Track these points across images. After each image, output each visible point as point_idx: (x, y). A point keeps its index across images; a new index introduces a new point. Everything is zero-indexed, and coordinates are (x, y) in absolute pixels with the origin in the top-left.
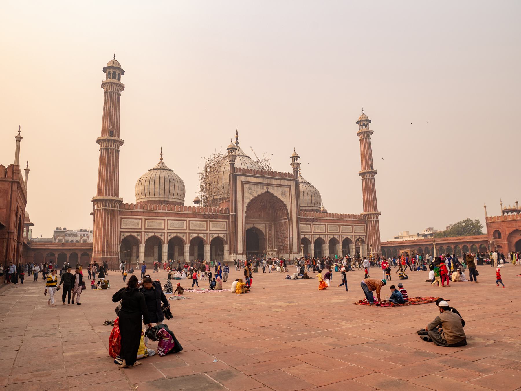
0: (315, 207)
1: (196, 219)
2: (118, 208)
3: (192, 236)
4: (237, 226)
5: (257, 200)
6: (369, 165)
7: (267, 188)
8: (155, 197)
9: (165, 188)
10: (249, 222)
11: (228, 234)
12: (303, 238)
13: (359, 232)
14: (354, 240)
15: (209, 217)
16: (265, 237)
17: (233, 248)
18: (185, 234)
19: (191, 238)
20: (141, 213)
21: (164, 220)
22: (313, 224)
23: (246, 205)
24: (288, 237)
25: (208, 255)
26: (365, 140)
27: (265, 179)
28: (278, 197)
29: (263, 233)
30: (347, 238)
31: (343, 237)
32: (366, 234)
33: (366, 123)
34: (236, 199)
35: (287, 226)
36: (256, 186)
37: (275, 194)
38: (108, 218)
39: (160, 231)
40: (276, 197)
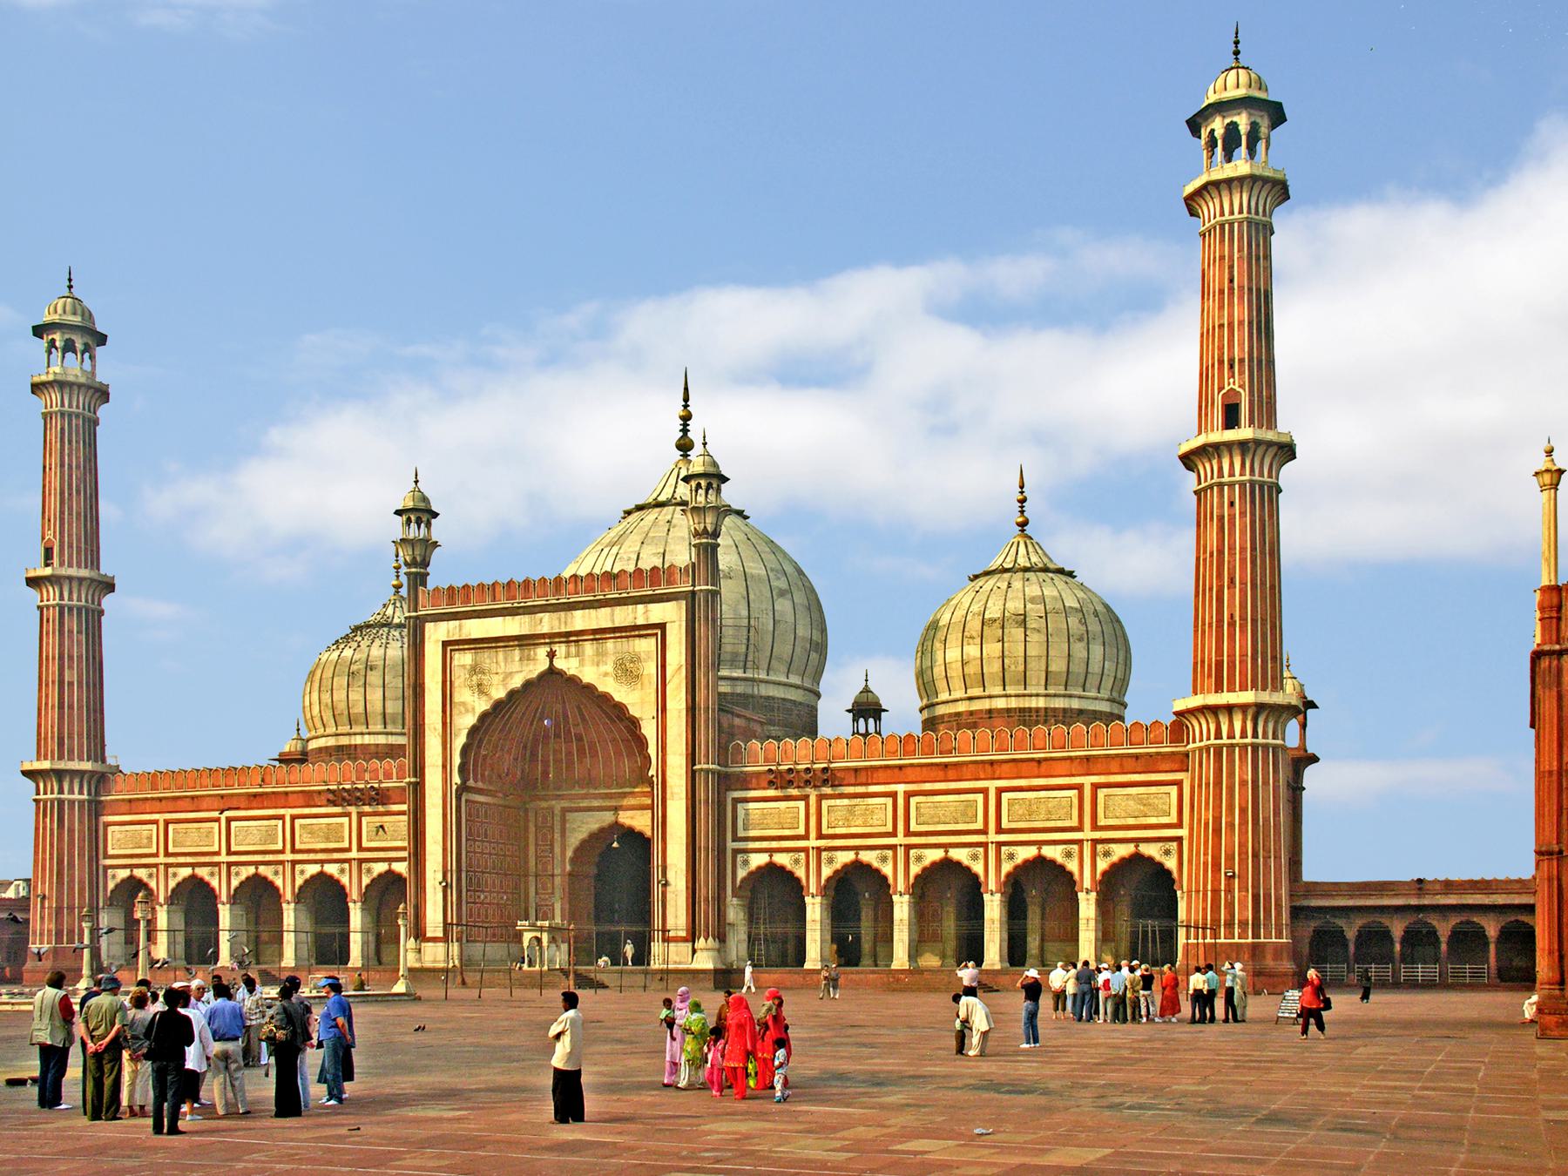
0: (1006, 696)
2: (81, 792)
7: (551, 655)
10: (596, 803)
12: (759, 868)
13: (1131, 821)
14: (1086, 872)
15: (344, 799)
20: (154, 802)
22: (821, 798)
23: (460, 741)
28: (600, 690)
30: (1040, 861)
31: (1011, 856)
32: (1183, 833)
37: (588, 675)
38: (45, 828)
40: (590, 689)
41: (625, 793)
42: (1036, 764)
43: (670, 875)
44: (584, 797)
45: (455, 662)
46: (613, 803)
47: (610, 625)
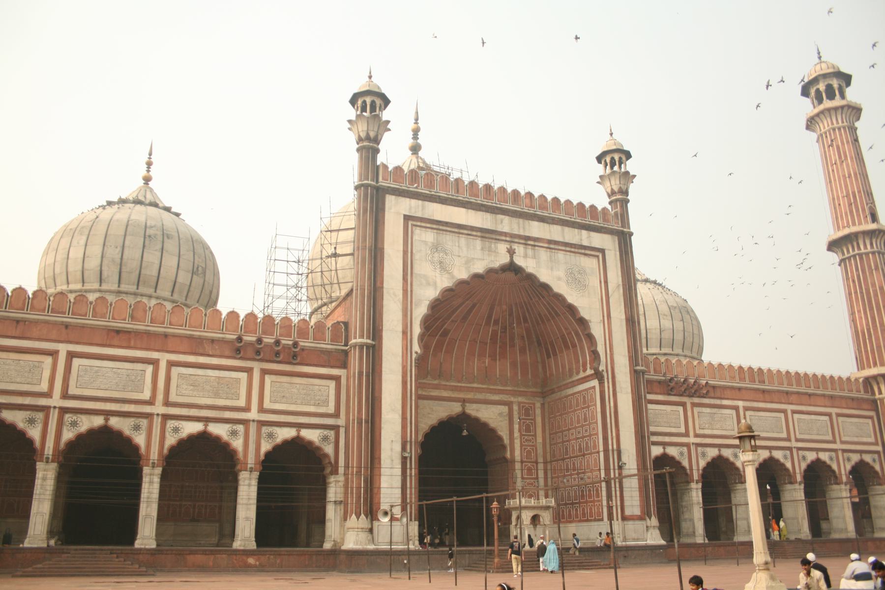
1: (202, 360)
3: (176, 430)
4: (377, 394)
5: (474, 306)
6: (863, 210)
7: (511, 252)
8: (84, 288)
9: (125, 257)
10: (445, 394)
11: (342, 431)
13: (856, 439)
14: (843, 468)
16: (508, 455)
17: (359, 488)
18: (144, 422)
19: (171, 440)
21: (54, 354)
22: (694, 405)
23: (421, 311)
24: (598, 452)
25: (247, 519)
26: (841, 135)
27: (500, 217)
29: (500, 439)
30: (818, 460)
31: (804, 458)
33: (835, 83)
34: (378, 284)
35: (595, 405)
36: (463, 240)
37: (544, 276)
39: (27, 401)
40: (546, 287)
41: (473, 388)
42: (807, 396)
43: (624, 459)
44: (437, 387)
45: (416, 237)
46: (462, 395)
47: (561, 240)
